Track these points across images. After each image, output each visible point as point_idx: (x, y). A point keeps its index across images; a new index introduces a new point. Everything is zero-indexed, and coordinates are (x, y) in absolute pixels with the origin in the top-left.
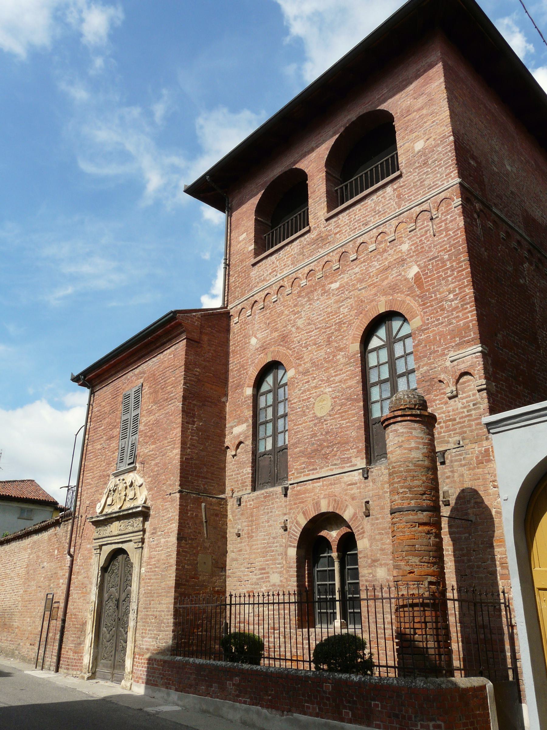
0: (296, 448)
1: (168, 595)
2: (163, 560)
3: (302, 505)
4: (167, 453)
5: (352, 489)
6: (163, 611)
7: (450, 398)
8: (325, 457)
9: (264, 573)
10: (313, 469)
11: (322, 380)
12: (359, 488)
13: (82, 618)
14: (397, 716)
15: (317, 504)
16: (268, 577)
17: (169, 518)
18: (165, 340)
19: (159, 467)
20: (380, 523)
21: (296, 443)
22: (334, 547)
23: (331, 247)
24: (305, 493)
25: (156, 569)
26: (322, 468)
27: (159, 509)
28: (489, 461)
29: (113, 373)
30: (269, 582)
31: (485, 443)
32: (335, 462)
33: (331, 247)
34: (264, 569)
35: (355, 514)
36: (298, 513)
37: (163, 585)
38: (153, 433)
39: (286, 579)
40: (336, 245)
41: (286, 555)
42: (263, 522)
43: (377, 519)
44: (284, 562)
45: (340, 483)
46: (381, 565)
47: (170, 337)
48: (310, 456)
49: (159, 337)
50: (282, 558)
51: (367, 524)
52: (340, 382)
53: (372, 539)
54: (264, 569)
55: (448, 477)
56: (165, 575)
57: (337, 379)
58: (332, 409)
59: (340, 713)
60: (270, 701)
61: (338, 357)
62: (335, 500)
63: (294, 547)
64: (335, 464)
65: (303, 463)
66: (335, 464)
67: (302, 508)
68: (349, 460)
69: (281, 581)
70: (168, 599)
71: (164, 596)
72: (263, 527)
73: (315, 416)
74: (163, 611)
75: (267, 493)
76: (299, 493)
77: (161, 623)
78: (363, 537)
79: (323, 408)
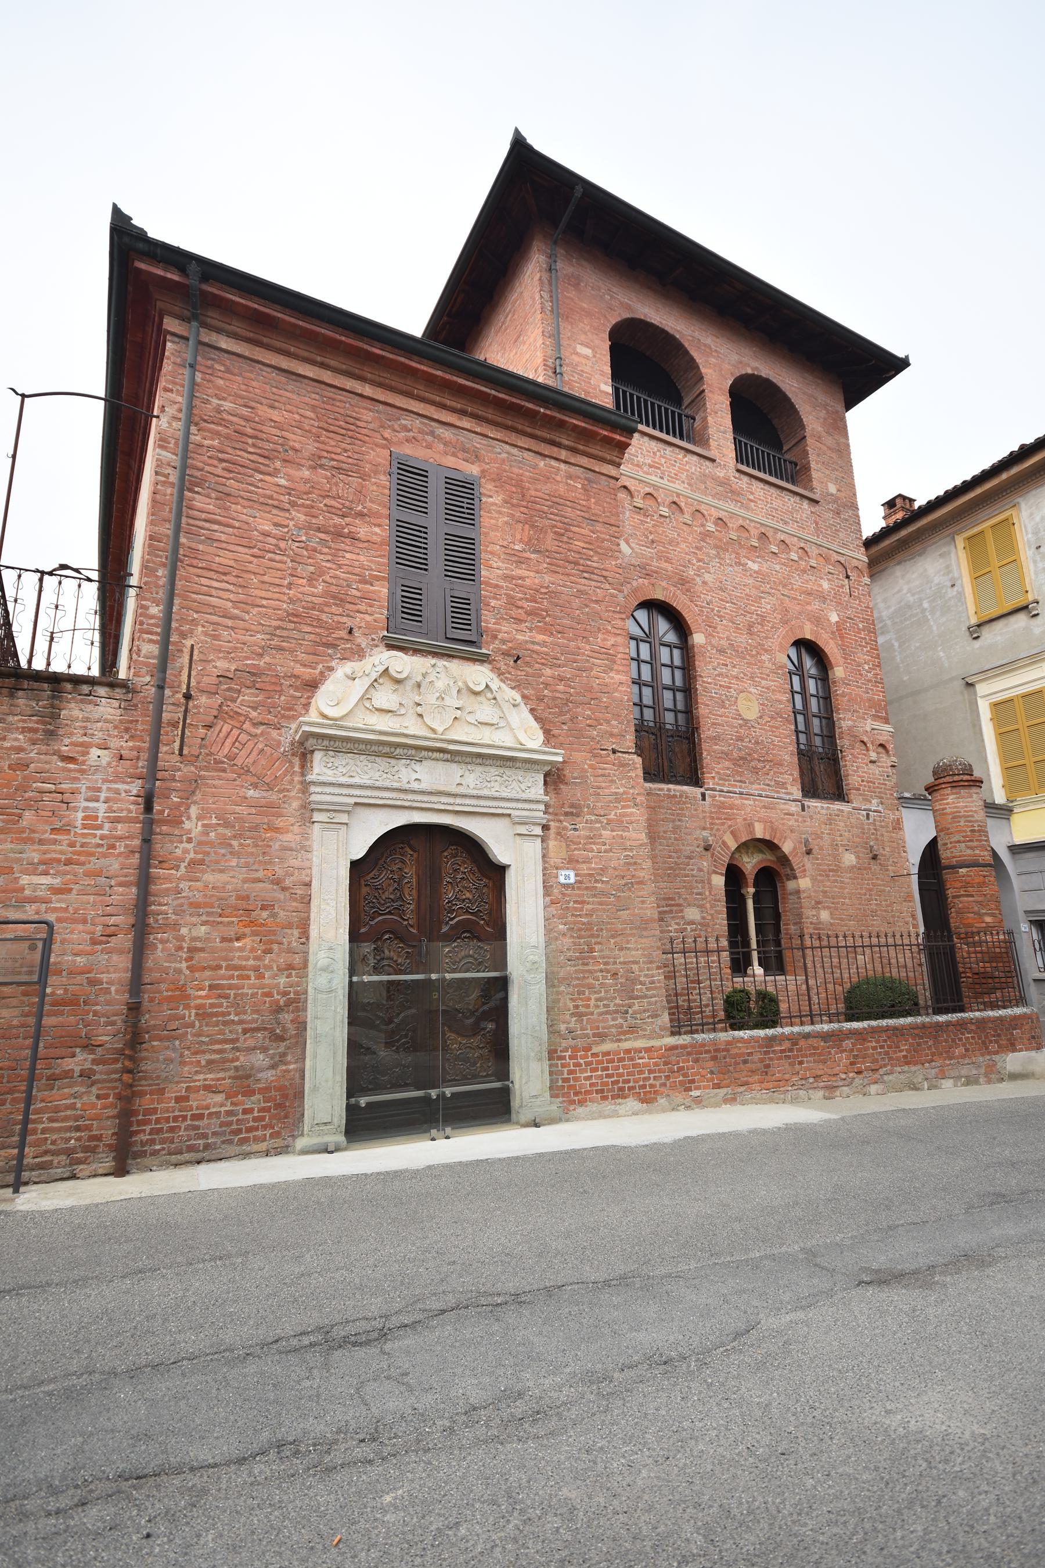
0: (716, 744)
1: (645, 933)
2: (615, 869)
3: (730, 823)
4: (592, 669)
5: (789, 820)
6: (637, 963)
7: (871, 762)
8: (755, 771)
9: (673, 905)
10: (741, 781)
11: (745, 675)
12: (797, 821)
13: (269, 994)
14: (1033, 1037)
15: (750, 826)
16: (682, 911)
17: (616, 794)
18: (566, 442)
19: (570, 686)
20: (820, 864)
21: (715, 738)
22: (751, 879)
23: (742, 512)
24: (732, 809)
25: (599, 885)
26: (752, 783)
27: (584, 770)
28: (900, 829)
29: (333, 363)
30: (683, 917)
31: (897, 813)
32: (767, 782)
33: (742, 512)
34: (672, 899)
35: (795, 849)
36: (725, 832)
37: (624, 914)
38: (542, 610)
39: (712, 915)
40: (748, 515)
41: (710, 883)
42: (665, 832)
43: (817, 859)
44: (707, 893)
45: (775, 809)
46: (824, 908)
47: (581, 447)
48: (735, 762)
49: (531, 416)
50: (703, 888)
51: (808, 863)
52: (768, 688)
53: (813, 879)
54: (672, 899)
55: (873, 834)
56: (629, 897)
57: (763, 682)
58: (761, 717)
59: (987, 1048)
60: (905, 1057)
61: (763, 657)
62: (772, 828)
63: (721, 874)
64: (768, 785)
65: (728, 769)
66: (768, 785)
67: (730, 826)
68: (783, 785)
69: (703, 918)
70: (644, 940)
71: (633, 935)
72: (665, 838)
73: (740, 715)
74: (637, 963)
75: (669, 790)
76: (722, 806)
77: (634, 983)
78: (805, 876)
79: (749, 709)
